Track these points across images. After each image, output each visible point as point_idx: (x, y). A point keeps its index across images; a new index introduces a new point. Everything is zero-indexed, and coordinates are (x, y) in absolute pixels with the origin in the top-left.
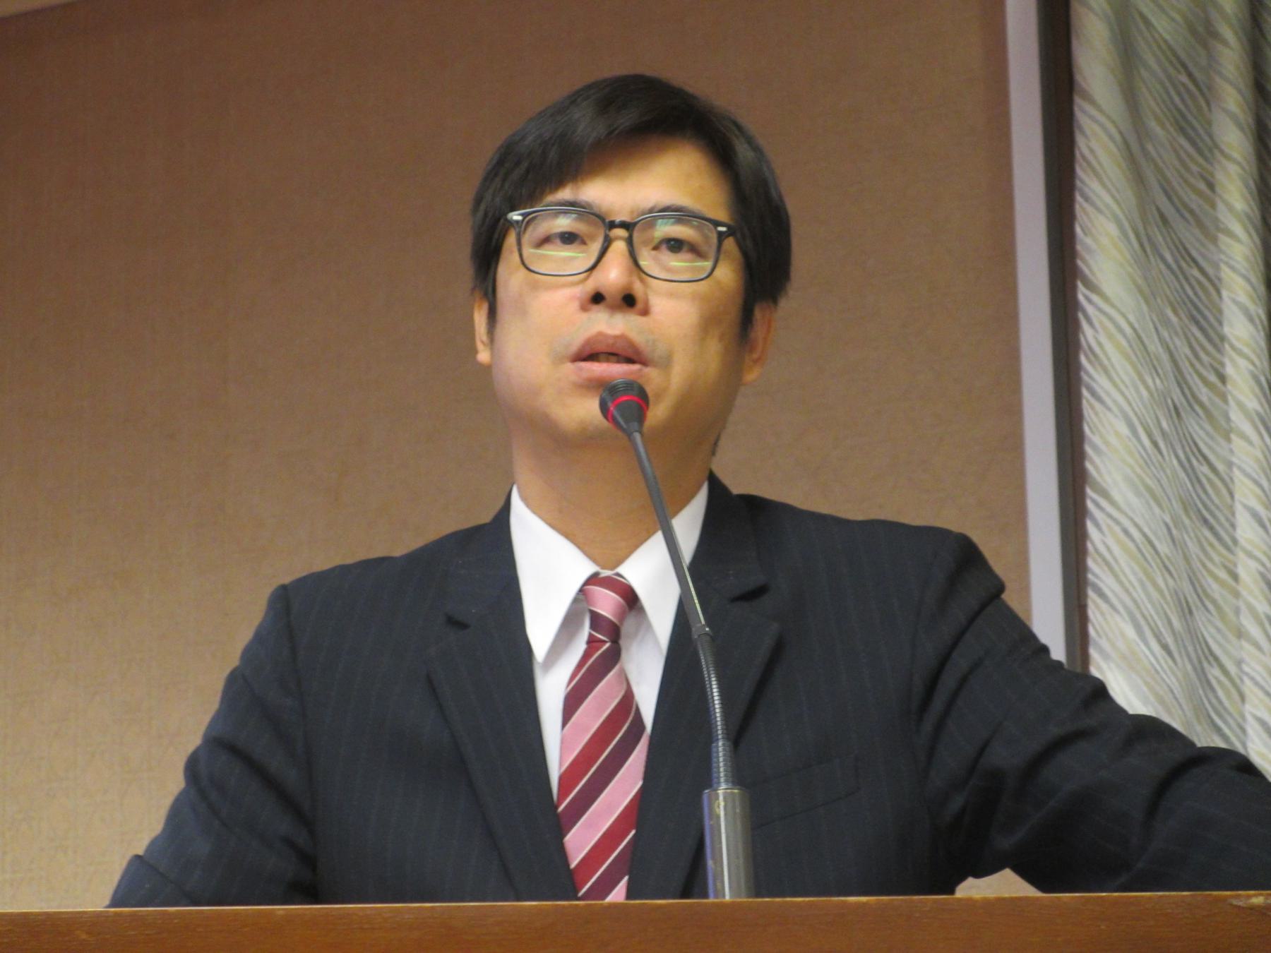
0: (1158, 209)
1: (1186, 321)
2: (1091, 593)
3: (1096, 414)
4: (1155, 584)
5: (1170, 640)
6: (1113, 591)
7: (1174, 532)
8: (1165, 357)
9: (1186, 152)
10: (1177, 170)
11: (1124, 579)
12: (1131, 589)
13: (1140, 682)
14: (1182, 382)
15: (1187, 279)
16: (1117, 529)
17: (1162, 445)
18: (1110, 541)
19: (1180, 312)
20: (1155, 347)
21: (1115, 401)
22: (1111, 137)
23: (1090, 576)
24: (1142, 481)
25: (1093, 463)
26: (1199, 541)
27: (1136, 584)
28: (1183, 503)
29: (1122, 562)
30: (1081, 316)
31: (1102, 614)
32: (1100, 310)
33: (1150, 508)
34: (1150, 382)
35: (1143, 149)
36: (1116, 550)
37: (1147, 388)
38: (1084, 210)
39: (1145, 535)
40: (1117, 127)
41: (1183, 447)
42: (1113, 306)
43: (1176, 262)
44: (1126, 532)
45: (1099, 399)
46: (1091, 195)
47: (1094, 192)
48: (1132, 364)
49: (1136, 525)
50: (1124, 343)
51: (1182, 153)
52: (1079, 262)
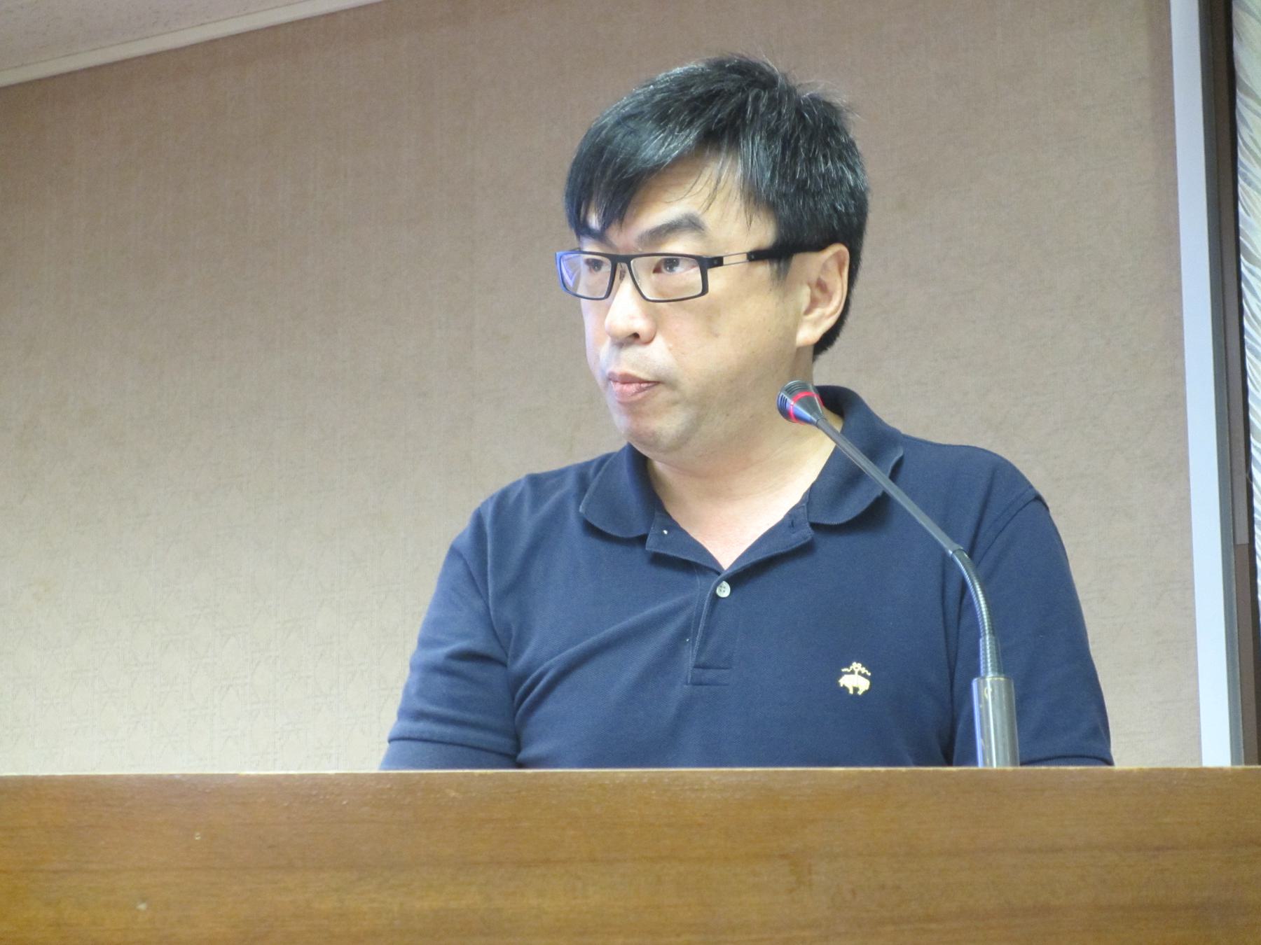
38: (1247, 193)
46: (1254, 180)
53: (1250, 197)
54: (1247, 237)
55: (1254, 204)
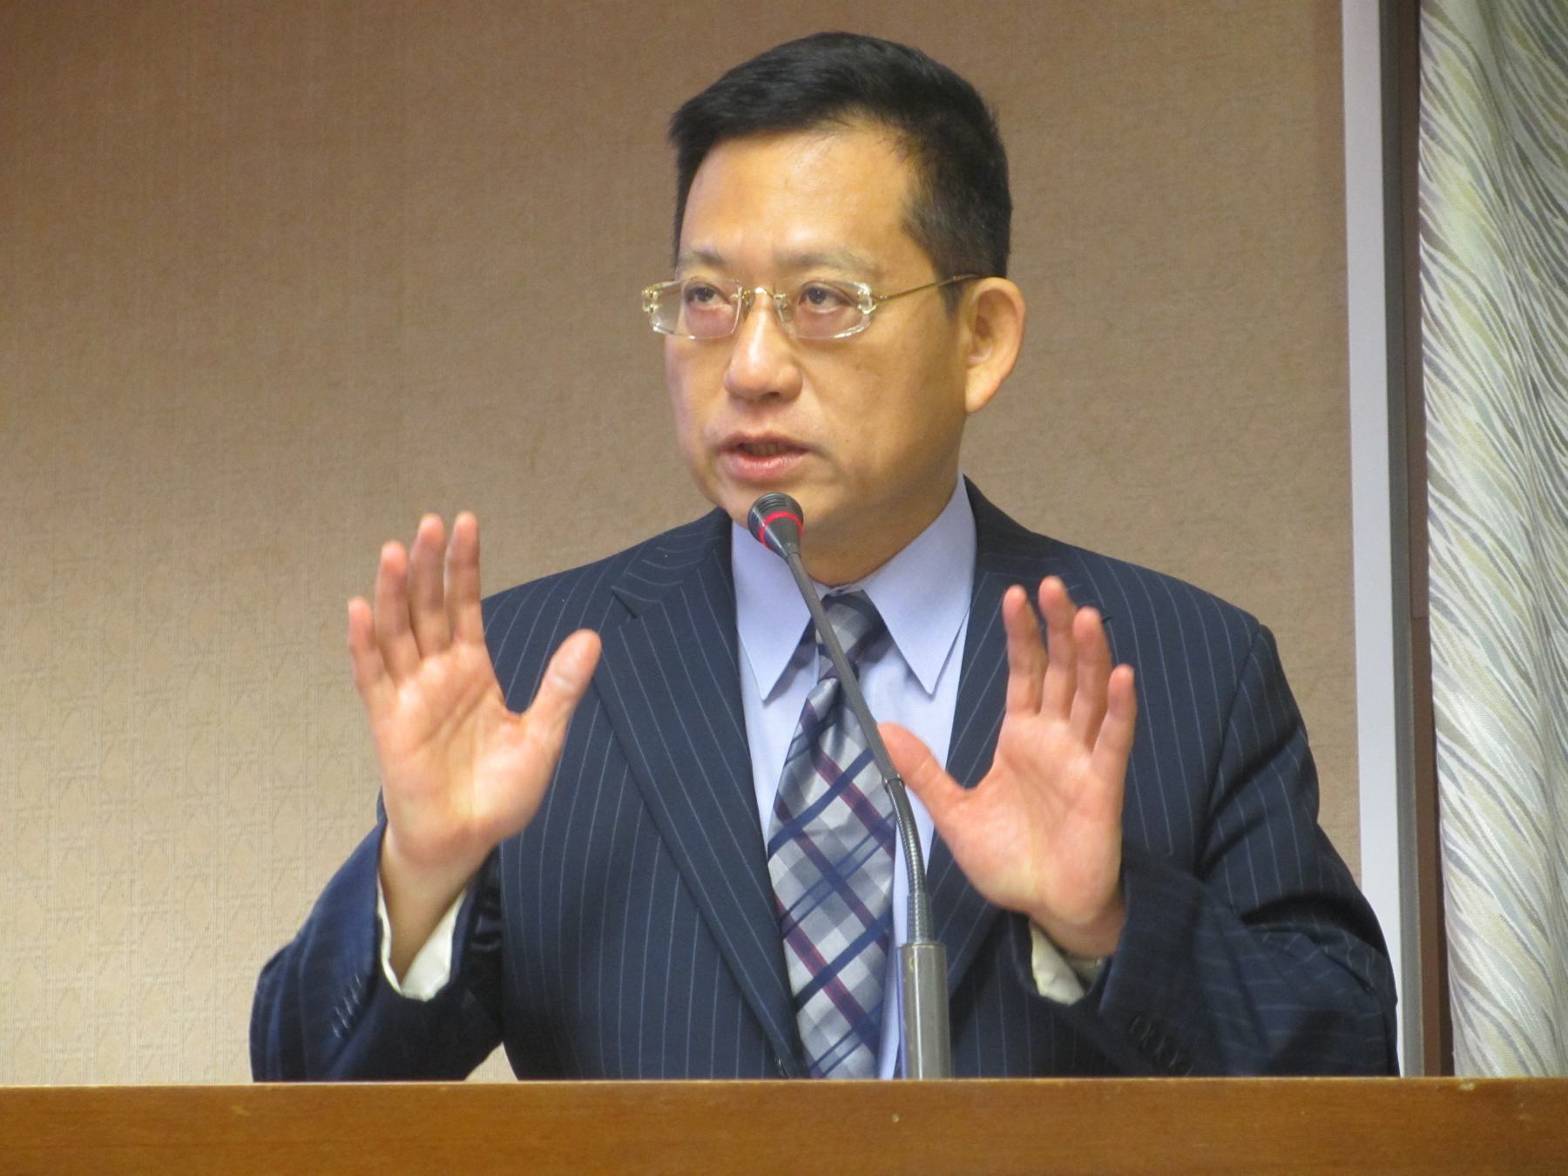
0: (1517, 145)
2: (1434, 613)
3: (1440, 396)
5: (1529, 667)
8: (1524, 326)
9: (1554, 77)
10: (1542, 99)
11: (1475, 597)
12: (1483, 608)
13: (1495, 717)
14: (1542, 357)
15: (1550, 232)
16: (1466, 536)
17: (1520, 433)
18: (1457, 550)
20: (1511, 313)
21: (1463, 382)
22: (1464, 61)
23: (1431, 589)
24: (1497, 478)
26: (1559, 547)
28: (1541, 501)
29: (1472, 576)
30: (1422, 276)
31: (1449, 636)
32: (1446, 271)
33: (1506, 509)
35: (1502, 73)
37: (1502, 363)
39: (1498, 541)
40: (1472, 49)
42: (1462, 267)
43: (1538, 209)
44: (1475, 538)
45: (1445, 380)
46: (1438, 131)
47: (1440, 127)
49: (1488, 530)
50: (1475, 311)
51: (1547, 76)
52: (1421, 211)
53: (1434, 157)
54: (1427, 209)
55: (1438, 164)
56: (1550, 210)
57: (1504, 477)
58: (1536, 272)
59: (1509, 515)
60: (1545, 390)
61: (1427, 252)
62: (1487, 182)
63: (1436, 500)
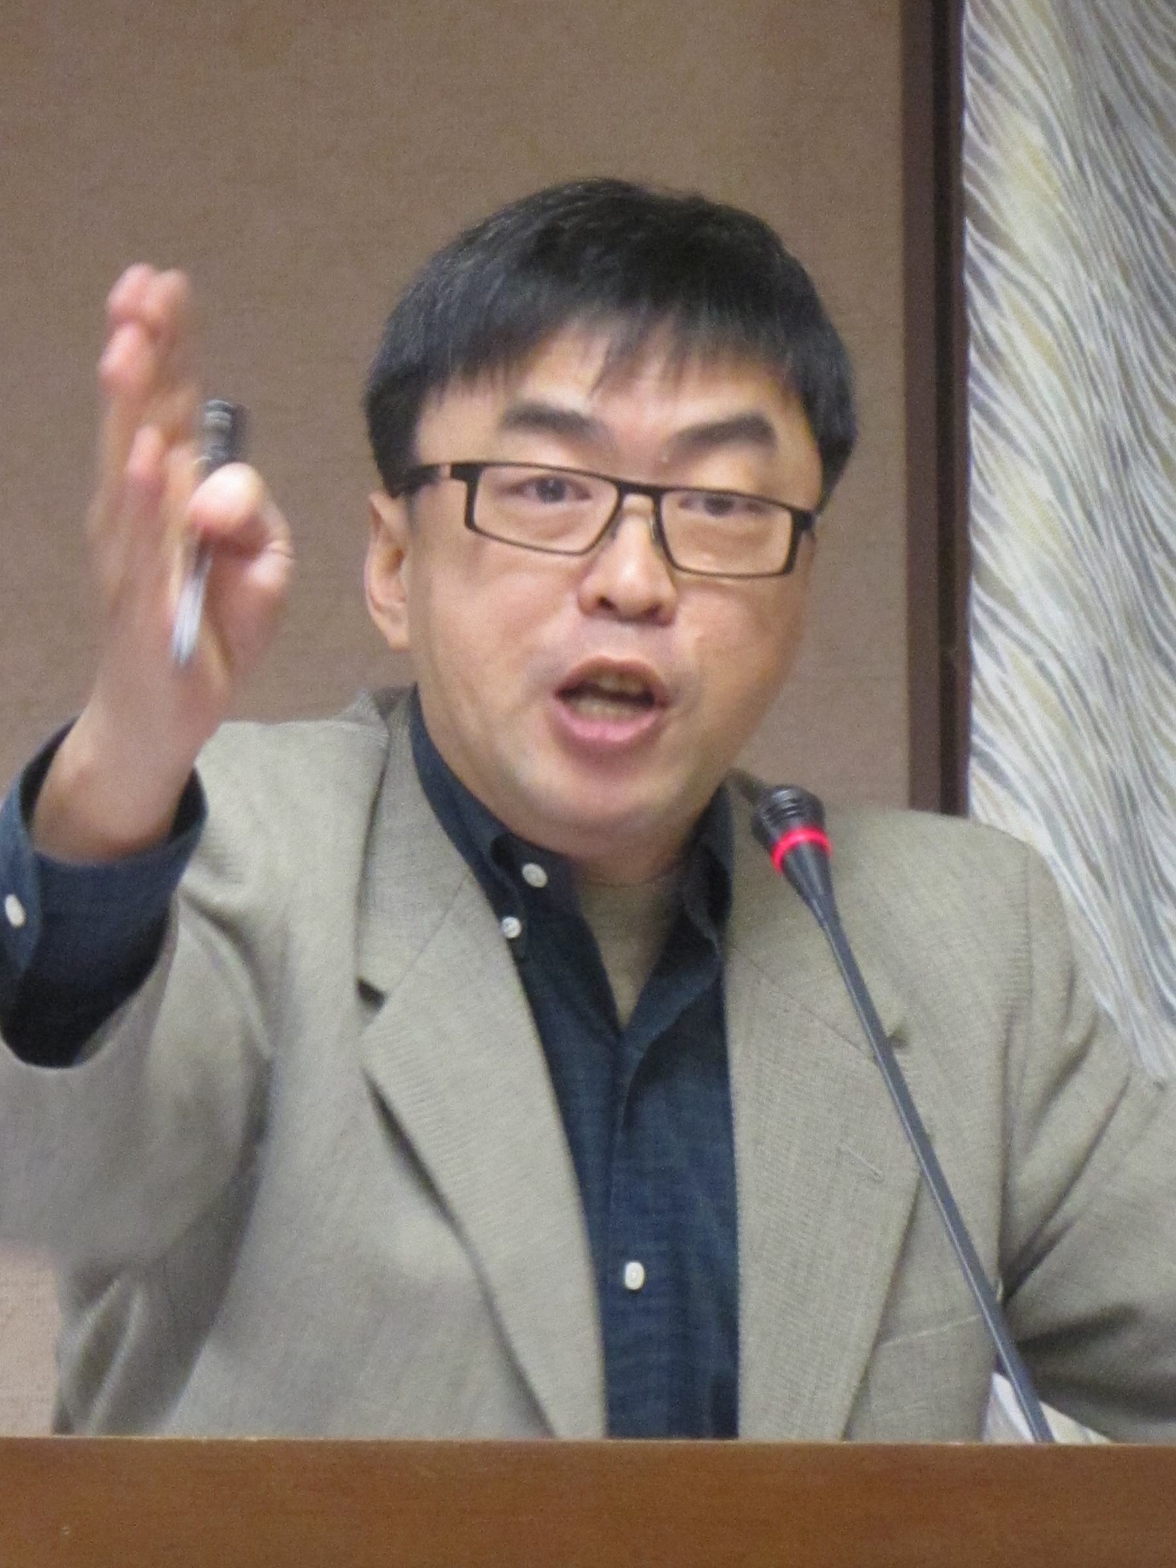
0: (1103, 97)
1: (1142, 298)
3: (998, 458)
4: (1081, 758)
6: (1016, 769)
7: (1113, 669)
12: (1047, 768)
14: (1132, 406)
16: (1028, 663)
19: (1135, 281)
25: (988, 543)
27: (1056, 760)
34: (1085, 406)
36: (1025, 699)
41: (1130, 520)
43: (1130, 190)
44: (1041, 667)
48: (1058, 369)
49: (1058, 656)
56: (1144, 192)
57: (1079, 581)
58: (1128, 283)
59: (1084, 638)
60: (1136, 458)
61: (979, 247)
62: (1064, 145)
63: (986, 609)
